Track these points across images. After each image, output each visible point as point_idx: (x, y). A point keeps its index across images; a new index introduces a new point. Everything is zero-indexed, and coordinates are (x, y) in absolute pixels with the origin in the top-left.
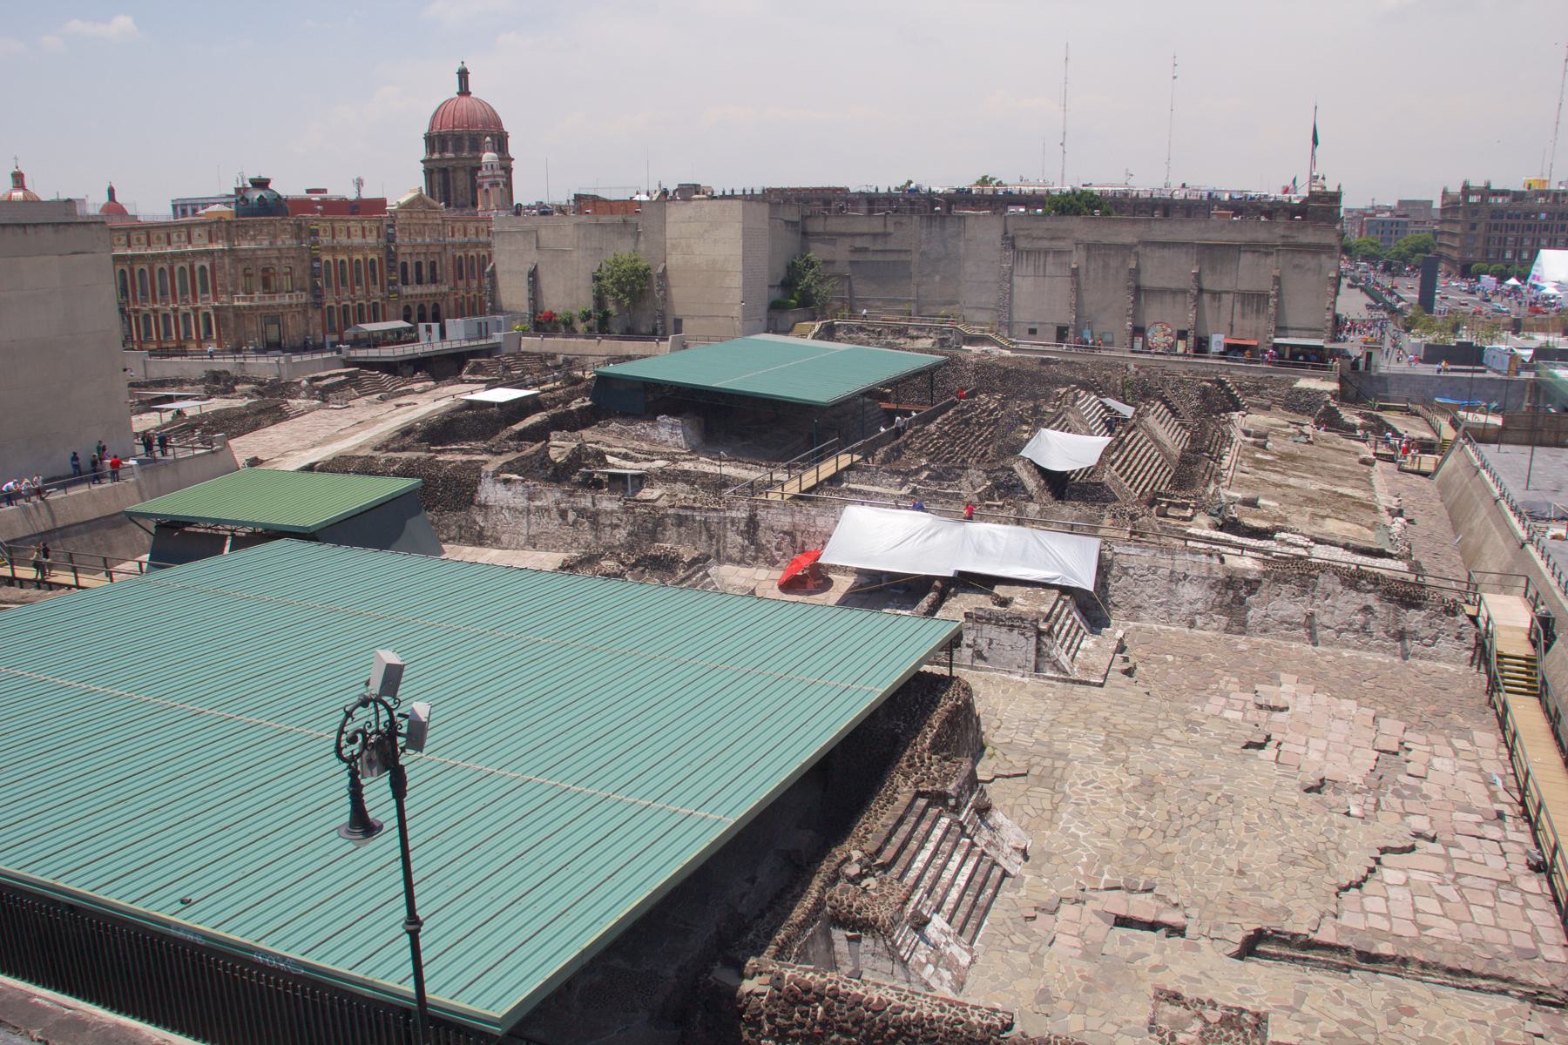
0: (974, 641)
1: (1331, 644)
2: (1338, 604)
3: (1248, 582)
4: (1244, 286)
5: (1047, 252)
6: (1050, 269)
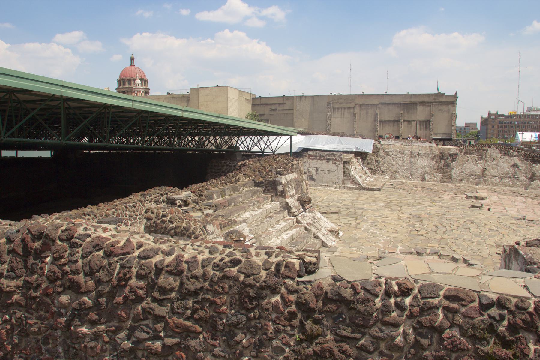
0: (308, 169)
1: (496, 185)
2: (499, 164)
3: (451, 155)
4: (420, 119)
5: (345, 108)
6: (346, 114)
